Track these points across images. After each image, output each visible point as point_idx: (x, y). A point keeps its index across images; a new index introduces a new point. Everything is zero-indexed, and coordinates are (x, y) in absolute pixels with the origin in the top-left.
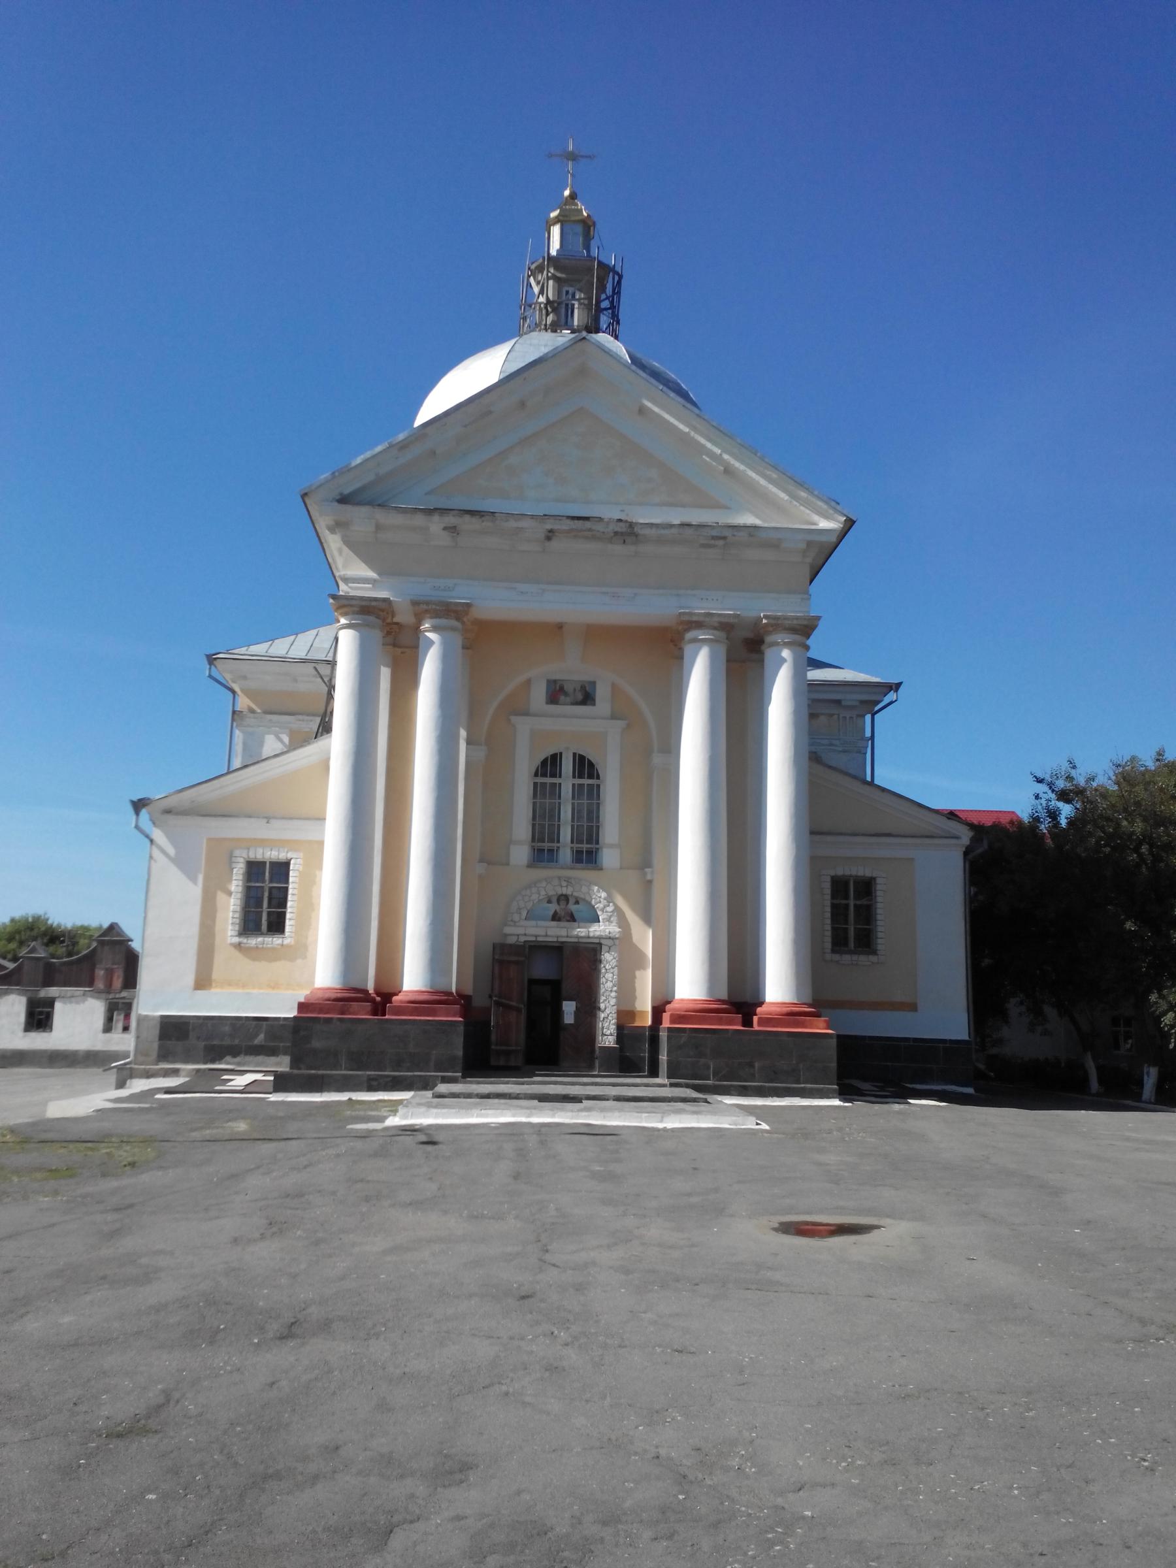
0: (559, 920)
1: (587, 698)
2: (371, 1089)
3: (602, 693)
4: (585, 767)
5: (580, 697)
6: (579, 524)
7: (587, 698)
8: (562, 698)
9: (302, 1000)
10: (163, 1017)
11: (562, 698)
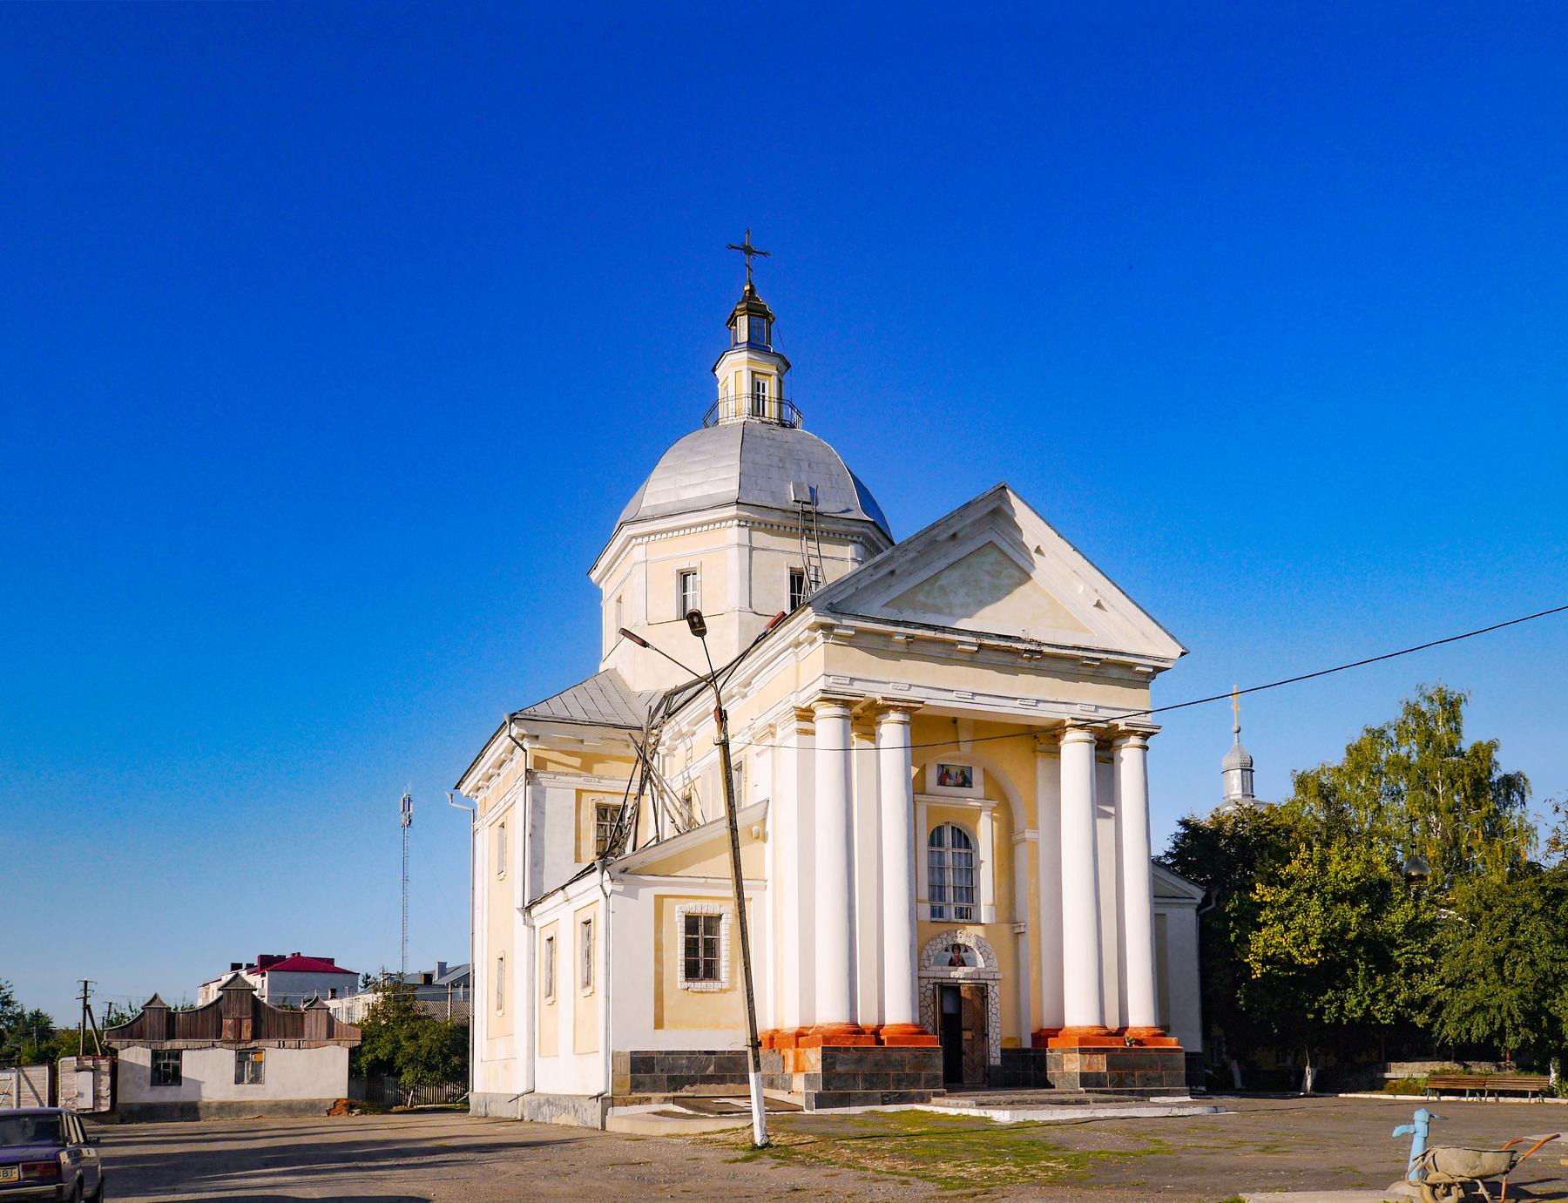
1: (966, 782)
2: (884, 1103)
3: (977, 777)
5: (960, 780)
7: (966, 782)
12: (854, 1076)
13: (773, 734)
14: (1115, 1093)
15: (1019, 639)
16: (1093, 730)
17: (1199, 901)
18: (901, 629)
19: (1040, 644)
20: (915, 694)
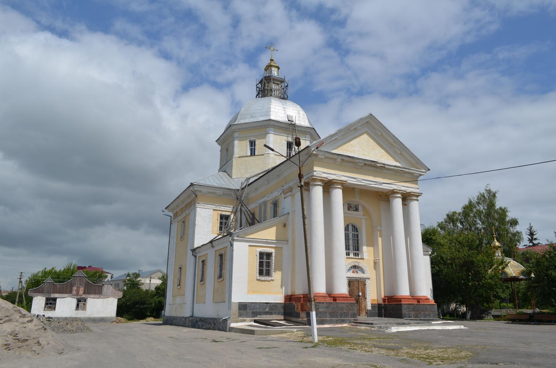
3: (360, 208)
6: (373, 164)
7: (357, 210)
12: (326, 313)
13: (291, 191)
14: (415, 320)
17: (430, 253)
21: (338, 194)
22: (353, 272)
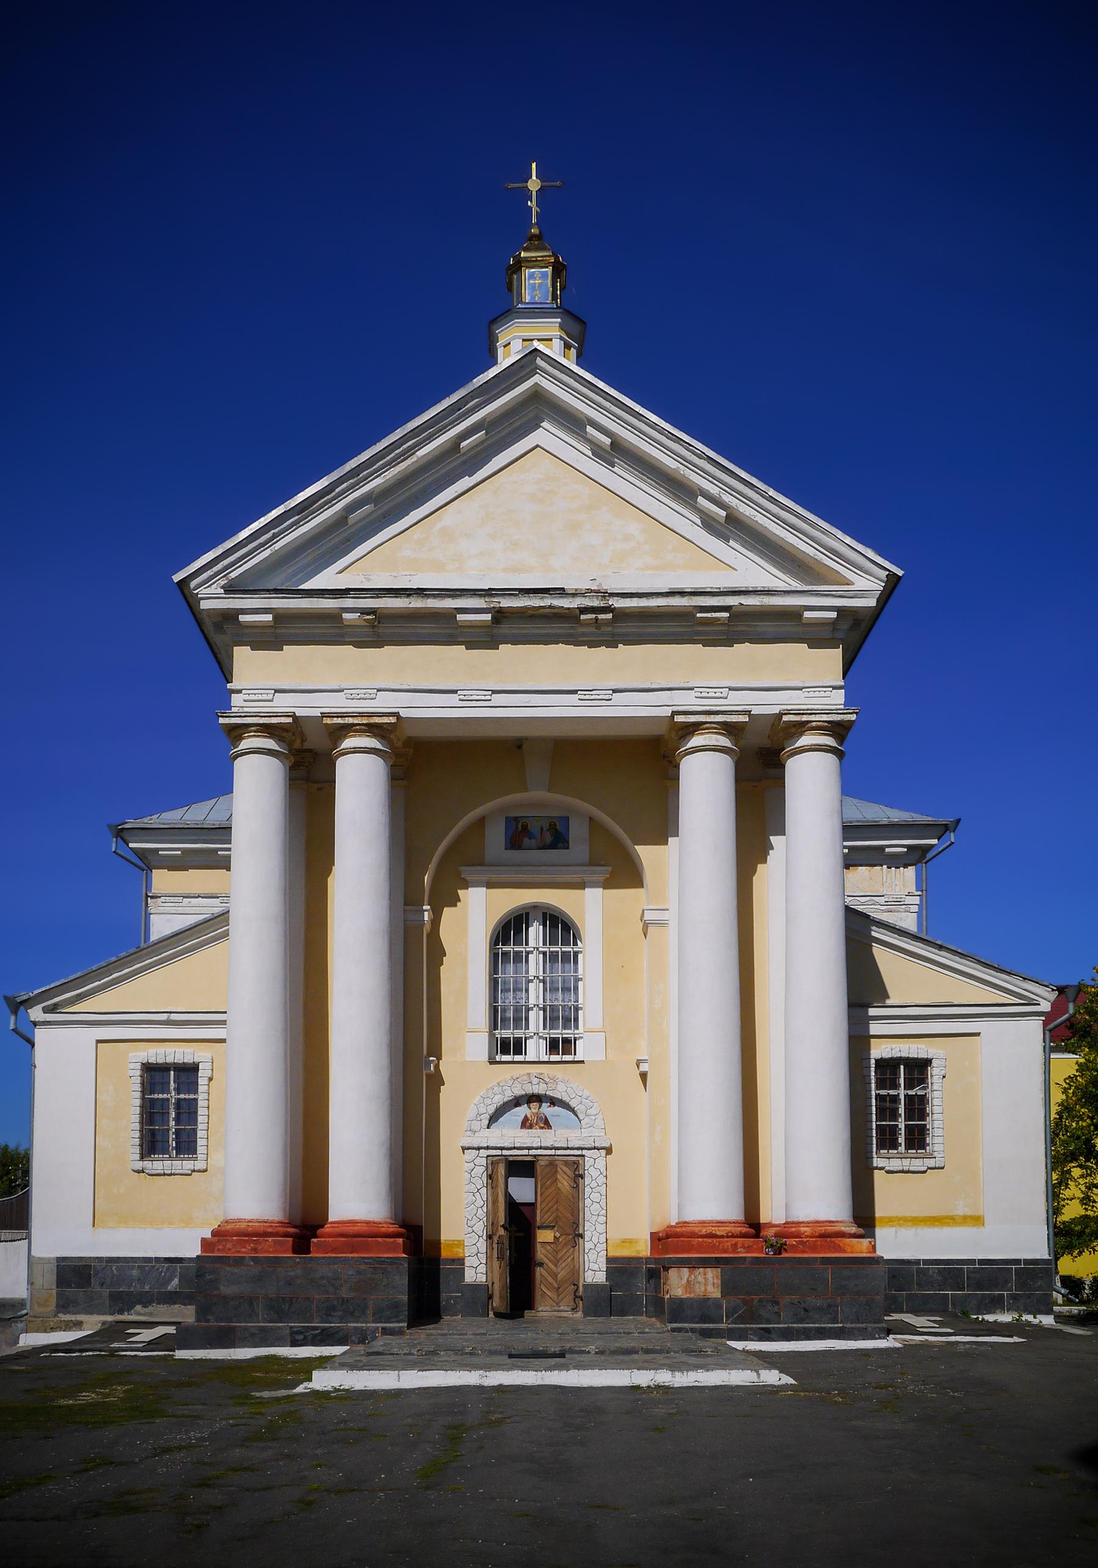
0: (531, 1127)
1: (558, 839)
2: (295, 1344)
3: (577, 831)
4: (560, 927)
5: (548, 838)
7: (558, 839)
8: (526, 841)
9: (208, 1235)
10: (59, 1259)
11: (526, 841)
12: (251, 1300)
15: (561, 592)
16: (729, 729)
17: (1045, 1006)
18: (349, 603)
19: (606, 595)
20: (386, 703)
21: (360, 784)
22: (526, 1124)
